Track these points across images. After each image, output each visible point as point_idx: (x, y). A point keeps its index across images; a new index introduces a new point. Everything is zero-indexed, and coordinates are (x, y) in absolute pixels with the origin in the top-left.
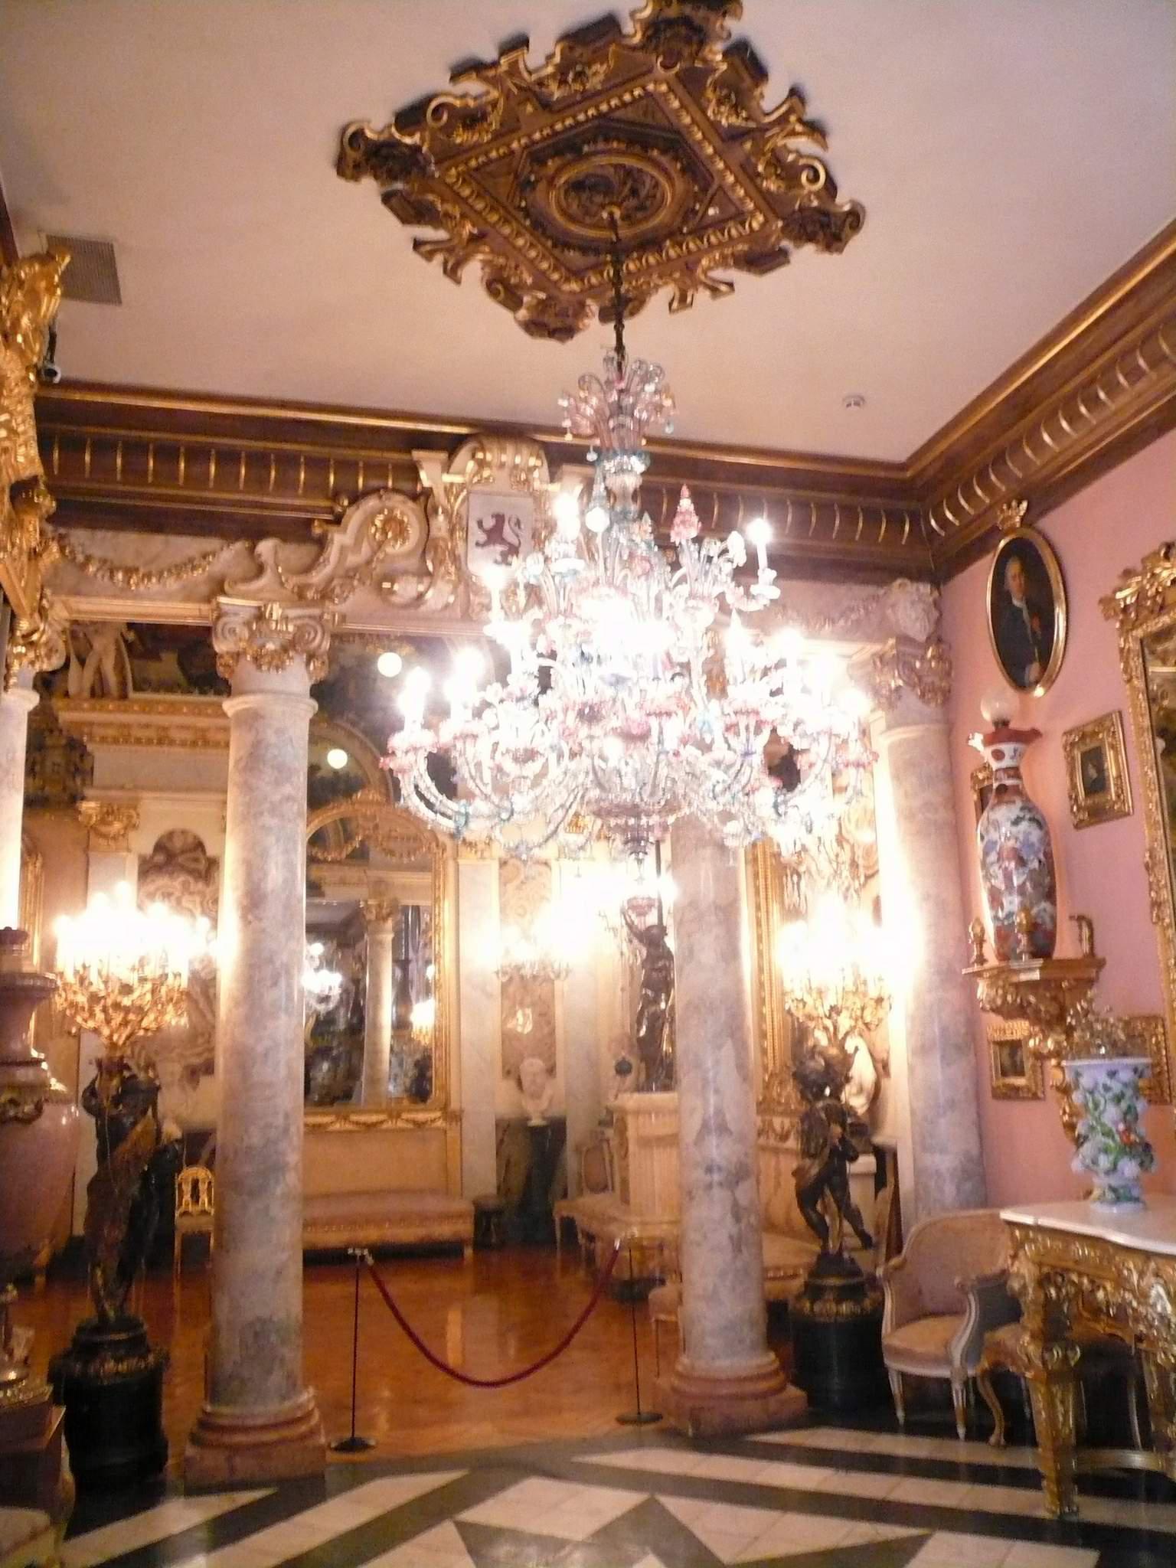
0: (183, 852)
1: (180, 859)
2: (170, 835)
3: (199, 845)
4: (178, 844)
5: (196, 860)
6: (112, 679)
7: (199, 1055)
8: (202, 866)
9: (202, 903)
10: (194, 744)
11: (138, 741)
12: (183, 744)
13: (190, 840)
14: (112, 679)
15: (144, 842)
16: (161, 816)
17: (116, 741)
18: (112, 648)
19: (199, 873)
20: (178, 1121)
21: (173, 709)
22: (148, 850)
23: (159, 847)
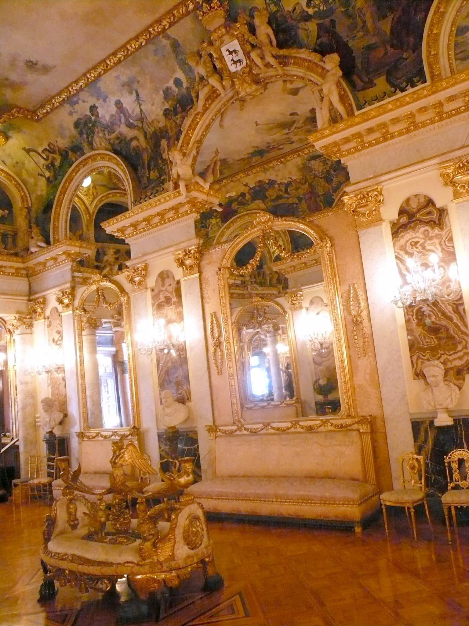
0: (419, 211)
1: (418, 216)
2: (408, 200)
3: (430, 202)
4: (414, 205)
5: (430, 213)
6: (340, 108)
7: (460, 358)
8: (435, 216)
9: (440, 244)
10: (408, 130)
11: (371, 144)
12: (401, 134)
13: (422, 200)
14: (340, 108)
15: (390, 212)
16: (397, 192)
17: (356, 150)
18: (334, 88)
19: (434, 222)
20: (449, 411)
21: (383, 111)
22: (394, 216)
23: (402, 212)
